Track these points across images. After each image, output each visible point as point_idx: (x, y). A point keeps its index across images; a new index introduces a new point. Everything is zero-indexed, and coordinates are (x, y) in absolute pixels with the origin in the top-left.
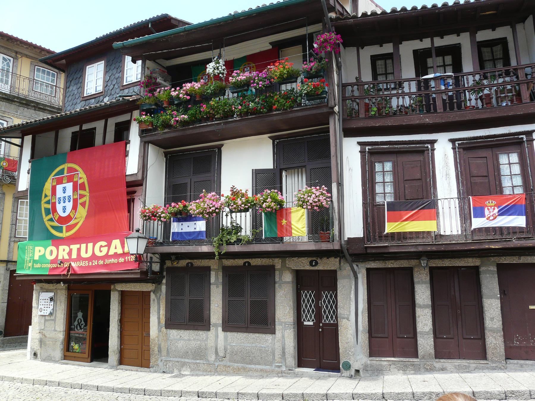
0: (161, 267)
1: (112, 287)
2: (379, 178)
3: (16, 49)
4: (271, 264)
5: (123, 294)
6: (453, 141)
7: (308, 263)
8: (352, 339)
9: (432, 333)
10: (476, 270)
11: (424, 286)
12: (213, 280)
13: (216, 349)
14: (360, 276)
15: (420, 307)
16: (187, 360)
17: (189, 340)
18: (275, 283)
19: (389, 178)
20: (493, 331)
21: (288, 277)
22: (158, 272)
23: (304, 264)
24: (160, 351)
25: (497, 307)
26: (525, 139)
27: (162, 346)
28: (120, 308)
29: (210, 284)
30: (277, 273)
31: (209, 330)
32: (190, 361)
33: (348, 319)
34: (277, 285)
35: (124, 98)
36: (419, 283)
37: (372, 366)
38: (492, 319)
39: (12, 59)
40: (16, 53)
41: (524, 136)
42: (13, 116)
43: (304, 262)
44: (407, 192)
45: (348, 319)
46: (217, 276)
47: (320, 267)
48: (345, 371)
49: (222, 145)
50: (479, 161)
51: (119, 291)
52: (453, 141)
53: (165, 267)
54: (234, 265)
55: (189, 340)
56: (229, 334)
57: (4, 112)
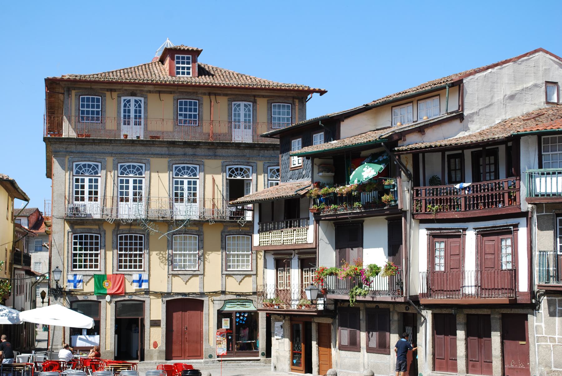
0: (335, 307)
1: (312, 320)
2: (437, 253)
5: (319, 325)
8: (424, 359)
9: (464, 357)
10: (487, 318)
11: (461, 326)
13: (364, 364)
15: (459, 340)
16: (350, 371)
17: (351, 358)
19: (443, 254)
22: (332, 311)
23: (403, 309)
24: (337, 365)
27: (338, 362)
28: (317, 335)
29: (360, 320)
30: (391, 314)
31: (360, 352)
34: (391, 322)
38: (495, 349)
39: (251, 104)
40: (255, 96)
41: (512, 227)
49: (363, 221)
50: (491, 243)
51: (316, 323)
53: (338, 306)
55: (351, 358)
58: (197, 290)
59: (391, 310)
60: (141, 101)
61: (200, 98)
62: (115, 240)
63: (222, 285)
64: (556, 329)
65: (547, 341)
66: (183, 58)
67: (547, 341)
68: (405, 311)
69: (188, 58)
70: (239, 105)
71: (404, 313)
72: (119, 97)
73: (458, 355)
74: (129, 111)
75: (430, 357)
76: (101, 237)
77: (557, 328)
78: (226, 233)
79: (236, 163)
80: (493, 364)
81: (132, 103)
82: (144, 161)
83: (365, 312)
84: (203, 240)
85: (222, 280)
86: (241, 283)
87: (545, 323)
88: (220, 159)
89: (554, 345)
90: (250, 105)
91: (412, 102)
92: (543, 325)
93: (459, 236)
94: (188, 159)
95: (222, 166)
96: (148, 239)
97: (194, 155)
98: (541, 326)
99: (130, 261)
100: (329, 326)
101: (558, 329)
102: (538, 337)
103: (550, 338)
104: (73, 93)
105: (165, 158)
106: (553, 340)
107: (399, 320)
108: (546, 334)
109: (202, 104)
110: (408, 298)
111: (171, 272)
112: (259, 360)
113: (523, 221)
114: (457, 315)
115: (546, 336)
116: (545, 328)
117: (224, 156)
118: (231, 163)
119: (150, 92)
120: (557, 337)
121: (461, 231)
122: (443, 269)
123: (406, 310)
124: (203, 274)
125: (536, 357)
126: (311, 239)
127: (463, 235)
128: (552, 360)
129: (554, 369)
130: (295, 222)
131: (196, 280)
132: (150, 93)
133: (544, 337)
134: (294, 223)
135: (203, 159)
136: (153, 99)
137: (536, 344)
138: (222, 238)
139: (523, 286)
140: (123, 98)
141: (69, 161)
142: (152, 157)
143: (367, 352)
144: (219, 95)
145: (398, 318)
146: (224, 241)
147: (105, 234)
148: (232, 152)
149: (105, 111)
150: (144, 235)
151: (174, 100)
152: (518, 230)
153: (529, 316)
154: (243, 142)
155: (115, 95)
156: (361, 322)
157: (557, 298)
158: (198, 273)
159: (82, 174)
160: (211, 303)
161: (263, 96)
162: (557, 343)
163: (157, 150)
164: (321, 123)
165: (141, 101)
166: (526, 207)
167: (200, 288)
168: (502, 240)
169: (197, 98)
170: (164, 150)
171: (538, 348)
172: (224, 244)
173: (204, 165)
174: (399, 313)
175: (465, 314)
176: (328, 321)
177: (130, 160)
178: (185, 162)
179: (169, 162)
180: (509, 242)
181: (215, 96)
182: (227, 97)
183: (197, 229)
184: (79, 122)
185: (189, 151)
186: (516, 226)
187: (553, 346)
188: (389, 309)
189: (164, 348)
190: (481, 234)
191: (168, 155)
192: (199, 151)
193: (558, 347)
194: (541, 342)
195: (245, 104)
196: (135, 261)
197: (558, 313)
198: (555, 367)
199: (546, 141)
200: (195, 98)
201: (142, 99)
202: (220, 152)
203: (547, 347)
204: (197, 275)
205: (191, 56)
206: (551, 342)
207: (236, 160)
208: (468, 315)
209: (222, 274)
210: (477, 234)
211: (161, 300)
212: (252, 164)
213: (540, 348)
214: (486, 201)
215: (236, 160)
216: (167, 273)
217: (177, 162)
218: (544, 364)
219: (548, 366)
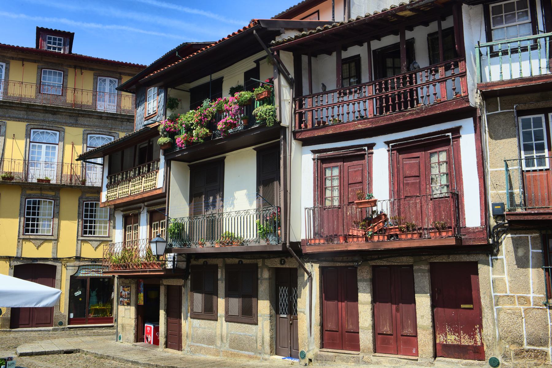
1: (161, 282)
2: (328, 183)
3: (120, 71)
4: (256, 262)
5: (169, 288)
6: (388, 143)
7: (279, 262)
9: (371, 328)
11: (365, 283)
12: (219, 276)
18: (257, 279)
19: (336, 183)
20: (424, 329)
21: (266, 274)
22: (185, 269)
23: (276, 263)
25: (427, 306)
26: (451, 137)
28: (166, 299)
29: (217, 280)
30: (259, 270)
33: (304, 313)
34: (259, 281)
35: (147, 126)
36: (361, 281)
37: (321, 356)
39: (117, 80)
40: (120, 73)
41: (450, 134)
42: (118, 131)
43: (276, 260)
44: (350, 196)
45: (304, 313)
46: (222, 272)
47: (287, 266)
48: (302, 360)
49: (225, 157)
50: (413, 161)
51: (165, 285)
52: (388, 143)
53: (191, 264)
54: (232, 263)
57: (111, 129)
58: (50, 256)
59: (260, 265)
63: (77, 250)
64: (529, 283)
65: (513, 303)
66: (55, 39)
67: (513, 303)
68: (279, 266)
69: (60, 40)
70: (105, 80)
71: (277, 269)
73: (360, 325)
77: (531, 281)
78: (84, 200)
79: (98, 132)
80: (419, 340)
83: (224, 270)
84: (59, 205)
85: (77, 246)
86: (97, 250)
88: (82, 127)
89: (527, 309)
90: (115, 81)
93: (362, 157)
97: (54, 122)
98: (502, 280)
100: (179, 288)
101: (533, 283)
102: (498, 298)
103: (519, 298)
105: (23, 121)
107: (270, 278)
108: (511, 291)
109: (67, 75)
110: (288, 245)
111: (22, 237)
112: (112, 326)
113: (467, 124)
115: (512, 294)
116: (510, 282)
118: (92, 132)
119: (13, 58)
120: (531, 295)
121: (366, 148)
122: (336, 203)
123: (281, 264)
124: (57, 240)
125: (494, 329)
126: (160, 182)
127: (369, 154)
128: (524, 332)
129: (526, 347)
130: (144, 168)
132: (13, 59)
133: (508, 296)
134: (143, 169)
138: (79, 204)
142: (8, 120)
143: (226, 321)
144: (86, 69)
145: (269, 276)
146: (81, 207)
148: (96, 121)
151: (38, 68)
152: (460, 137)
153: (479, 266)
154: (105, 111)
156: (220, 283)
157: (529, 236)
158: (52, 238)
160: (64, 269)
162: (532, 306)
163: (15, 113)
164: (178, 54)
167: (53, 253)
169: (62, 69)
170: (22, 114)
171: (498, 314)
173: (64, 132)
174: (270, 269)
176: (178, 282)
178: (45, 127)
179: (27, 126)
180: (443, 157)
181: (81, 69)
182: (93, 72)
183: (53, 194)
185: (50, 117)
186: (456, 131)
187: (525, 310)
188: (257, 264)
189: (9, 316)
192: (58, 118)
193: (535, 311)
194: (503, 304)
195: (110, 80)
197: (533, 258)
198: (529, 344)
200: (60, 69)
201: (4, 65)
202: (81, 120)
204: (50, 240)
205: (62, 38)
207: (98, 130)
208: (375, 269)
209: (78, 240)
211: (8, 264)
212: (114, 135)
213: (502, 315)
214: (409, 99)
215: (98, 130)
216: (17, 238)
217: (36, 127)
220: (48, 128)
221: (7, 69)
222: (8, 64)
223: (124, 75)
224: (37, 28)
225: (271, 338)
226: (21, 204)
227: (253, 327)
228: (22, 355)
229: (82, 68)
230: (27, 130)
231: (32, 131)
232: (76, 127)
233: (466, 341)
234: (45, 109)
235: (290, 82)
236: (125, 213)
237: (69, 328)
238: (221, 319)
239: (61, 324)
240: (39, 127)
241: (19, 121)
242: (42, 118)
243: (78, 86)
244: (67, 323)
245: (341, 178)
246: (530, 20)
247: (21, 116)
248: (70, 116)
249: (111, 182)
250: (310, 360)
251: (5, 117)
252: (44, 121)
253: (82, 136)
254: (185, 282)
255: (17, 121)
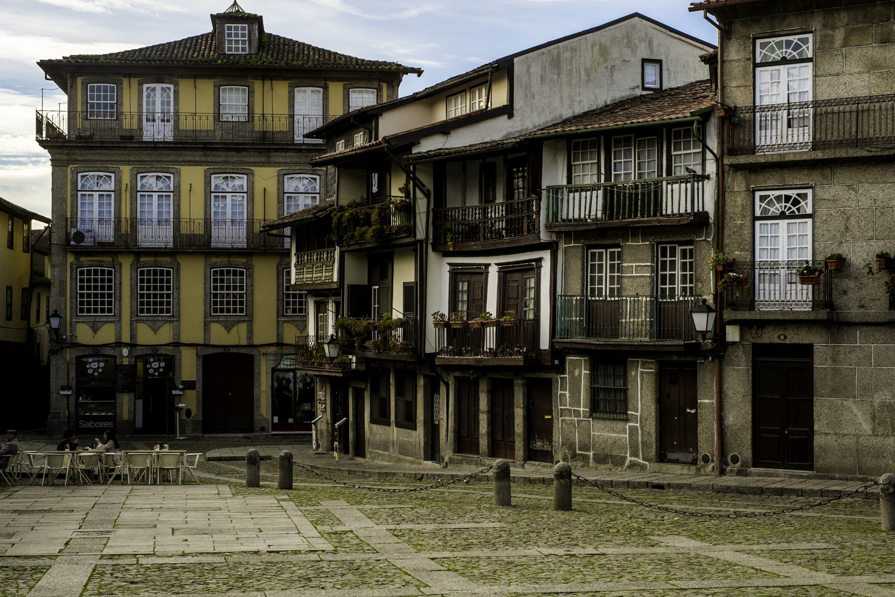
14: (450, 383)
19: (465, 298)
32: (381, 452)
39: (321, 90)
41: (534, 263)
52: (497, 264)
56: (399, 429)
58: (244, 342)
59: (418, 372)
60: (169, 89)
61: (250, 84)
62: (134, 276)
66: (236, 29)
67: (571, 416)
69: (243, 29)
70: (305, 91)
72: (140, 84)
74: (154, 103)
75: (451, 435)
76: (115, 271)
78: (284, 266)
81: (158, 92)
82: (172, 170)
84: (252, 275)
87: (570, 392)
91: (465, 91)
92: (567, 393)
94: (232, 167)
95: (278, 176)
96: (178, 275)
99: (155, 303)
103: (574, 410)
104: (79, 80)
105: (201, 165)
106: (577, 414)
107: (424, 386)
109: (253, 91)
114: (480, 380)
116: (570, 397)
117: (280, 163)
118: (290, 171)
120: (582, 409)
129: (578, 452)
131: (243, 327)
135: (252, 166)
136: (186, 86)
137: (560, 419)
138: (278, 273)
139: (545, 343)
140: (145, 86)
141: (72, 172)
142: (183, 165)
146: (281, 276)
147: (121, 267)
149: (122, 104)
150: (173, 268)
151: (215, 86)
155: (135, 82)
156: (391, 387)
157: (583, 359)
158: (247, 319)
159: (89, 188)
161: (338, 80)
165: (169, 89)
166: (544, 237)
168: (527, 278)
169: (247, 84)
170: (198, 156)
172: (280, 281)
173: (253, 174)
174: (425, 376)
175: (489, 378)
177: (153, 170)
179: (205, 171)
181: (271, 80)
183: (244, 260)
184: (87, 119)
185: (234, 157)
190: (504, 272)
191: (205, 162)
194: (565, 416)
196: (162, 303)
198: (580, 449)
199: (576, 147)
201: (172, 86)
203: (572, 423)
204: (244, 321)
205: (246, 25)
206: (575, 416)
207: (298, 168)
210: (499, 272)
211: (195, 351)
213: (564, 425)
215: (298, 168)
217: (216, 171)
218: (567, 445)
219: (572, 447)
220: (232, 171)
221: (176, 93)
222: (176, 85)
223: (330, 81)
224: (212, 15)
225: (425, 443)
226: (205, 276)
227: (413, 432)
228: (209, 459)
229: (272, 78)
230: (206, 177)
231: (213, 176)
232: (268, 166)
233: (547, 448)
234: (226, 146)
235: (427, 195)
236: (318, 299)
237: (273, 435)
238: (393, 424)
239: (263, 429)
240: (220, 171)
241: (196, 165)
242: (224, 159)
243: (268, 111)
244: (270, 429)
245: (468, 291)
246: (596, 161)
247: (197, 159)
248: (259, 152)
249: (298, 261)
250: (446, 463)
251: (178, 162)
252: (226, 162)
253: (276, 179)
254: (366, 385)
255: (193, 165)
